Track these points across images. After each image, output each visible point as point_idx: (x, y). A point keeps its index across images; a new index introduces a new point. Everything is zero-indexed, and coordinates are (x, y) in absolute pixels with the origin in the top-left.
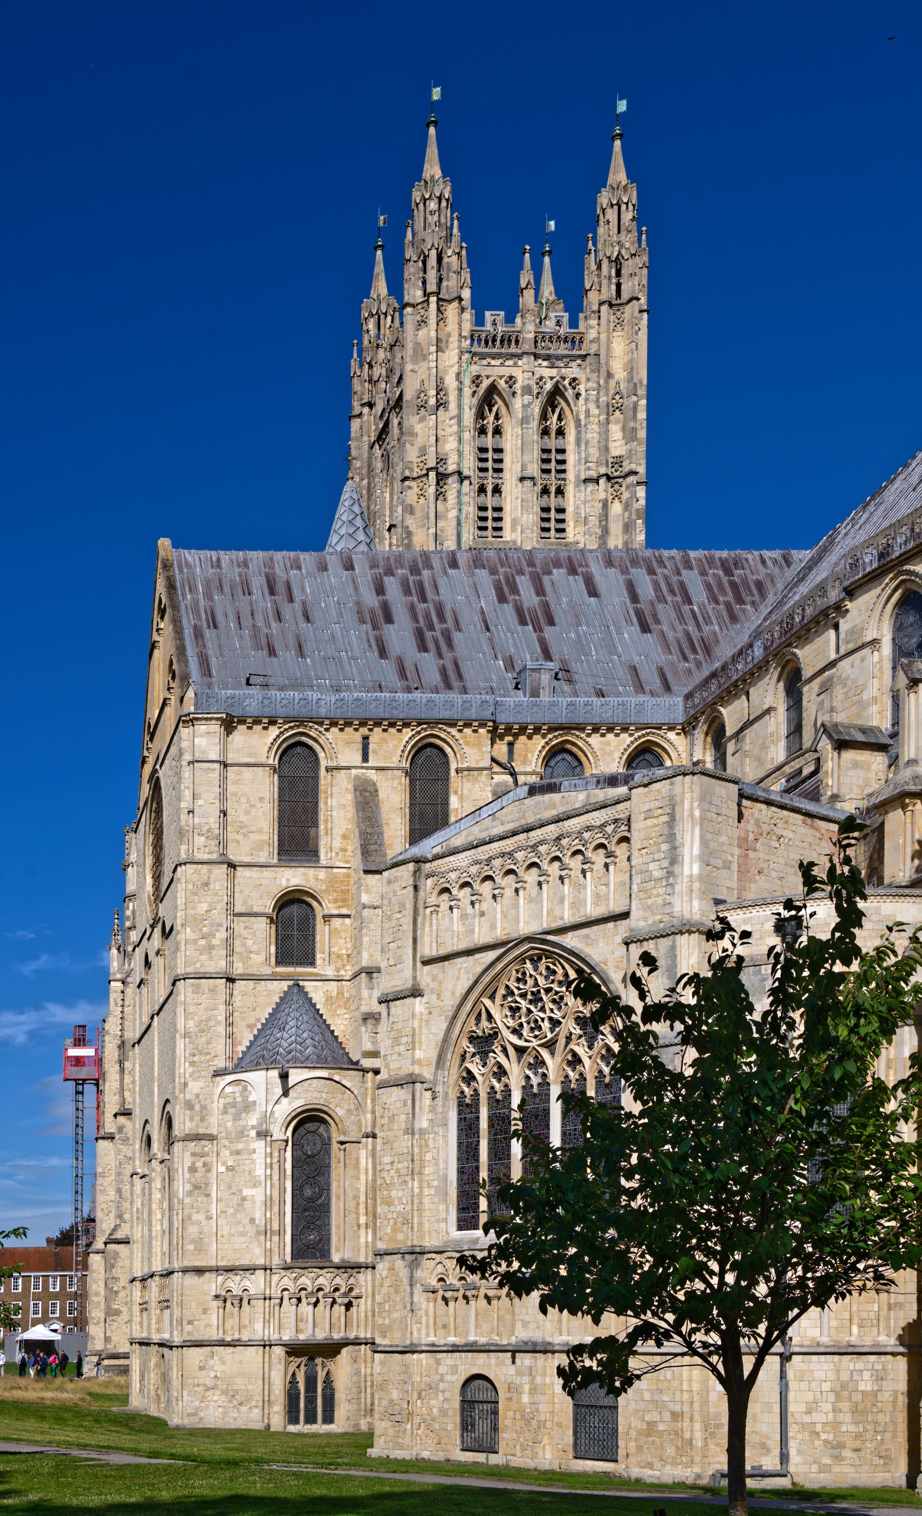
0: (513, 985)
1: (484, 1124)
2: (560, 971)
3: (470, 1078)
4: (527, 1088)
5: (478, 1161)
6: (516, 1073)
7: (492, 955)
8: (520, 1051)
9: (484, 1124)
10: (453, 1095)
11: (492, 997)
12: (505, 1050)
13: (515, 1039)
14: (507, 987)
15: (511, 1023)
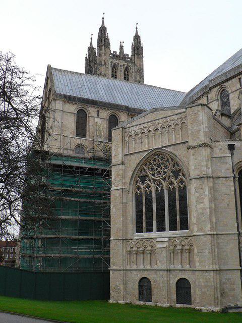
0: (152, 162)
1: (144, 201)
2: (165, 157)
3: (139, 188)
4: (157, 191)
5: (142, 212)
6: (153, 187)
7: (145, 154)
8: (154, 180)
9: (144, 201)
10: (134, 193)
11: (145, 165)
12: (150, 180)
13: (152, 177)
14: (150, 162)
15: (151, 172)
